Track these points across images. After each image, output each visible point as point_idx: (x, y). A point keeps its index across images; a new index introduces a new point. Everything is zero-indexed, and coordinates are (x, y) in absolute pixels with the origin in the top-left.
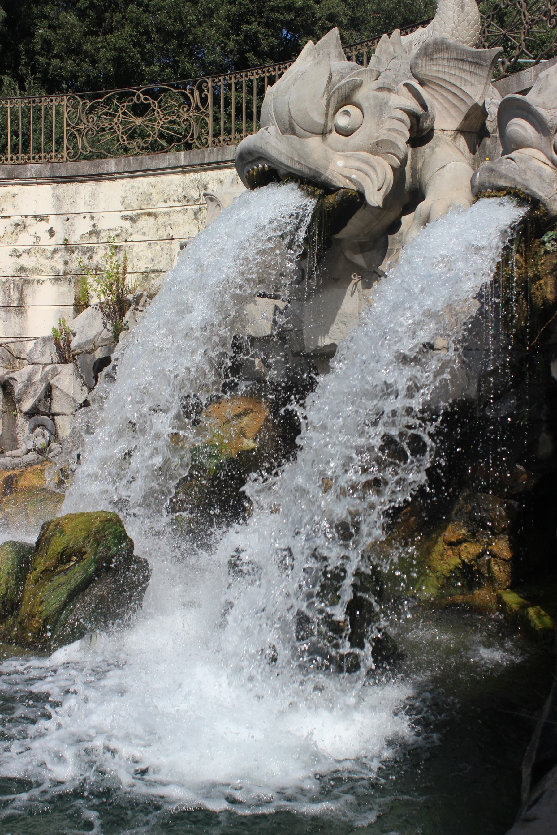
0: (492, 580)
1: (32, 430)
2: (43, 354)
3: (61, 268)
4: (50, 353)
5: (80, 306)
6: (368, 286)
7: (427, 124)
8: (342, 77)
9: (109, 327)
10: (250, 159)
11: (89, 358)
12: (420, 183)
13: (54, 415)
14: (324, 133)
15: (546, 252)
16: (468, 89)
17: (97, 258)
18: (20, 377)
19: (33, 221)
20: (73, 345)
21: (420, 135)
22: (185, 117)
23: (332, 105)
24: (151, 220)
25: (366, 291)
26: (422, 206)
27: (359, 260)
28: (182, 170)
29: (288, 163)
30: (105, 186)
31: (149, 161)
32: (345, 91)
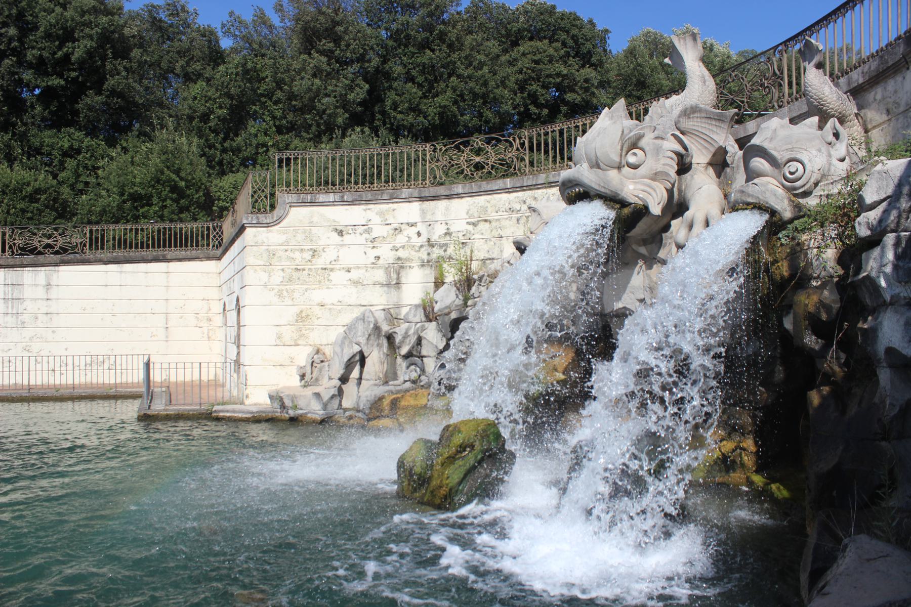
0: (743, 465)
1: (408, 367)
2: (415, 316)
3: (425, 257)
4: (420, 315)
5: (439, 283)
6: (650, 267)
7: (688, 160)
8: (631, 131)
9: (460, 297)
10: (570, 185)
11: (447, 318)
12: (684, 199)
13: (423, 357)
14: (619, 168)
15: (782, 245)
16: (715, 137)
17: (450, 251)
18: (400, 331)
20: (436, 309)
21: (684, 168)
22: (510, 155)
23: (625, 149)
24: (487, 224)
25: (649, 271)
26: (688, 214)
27: (643, 250)
28: (508, 191)
29: (597, 187)
30: (455, 202)
31: (485, 185)
32: (633, 140)
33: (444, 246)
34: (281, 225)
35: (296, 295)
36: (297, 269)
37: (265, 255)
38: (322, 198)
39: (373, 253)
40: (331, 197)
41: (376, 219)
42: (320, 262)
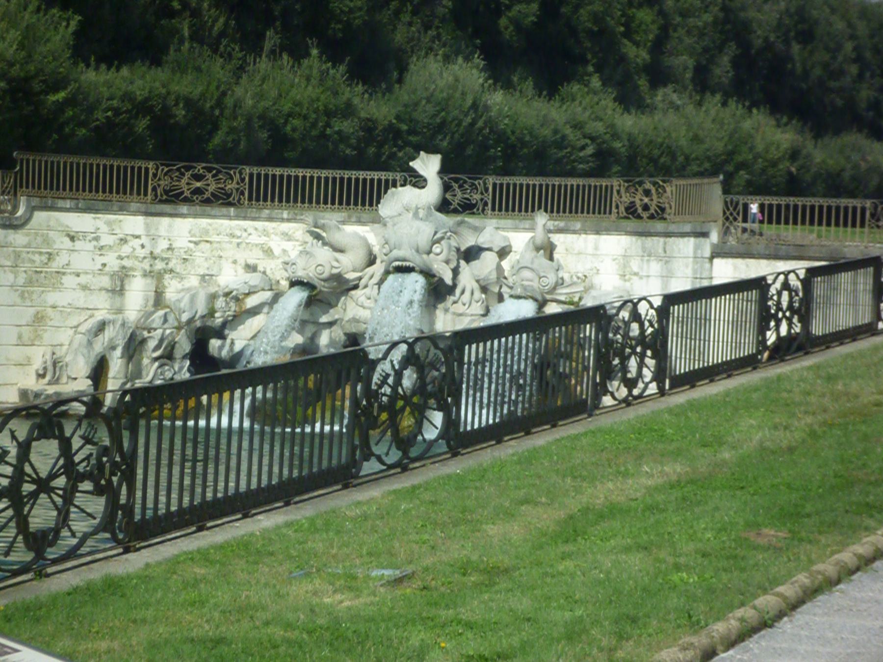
3: (147, 268)
16: (470, 239)
19: (132, 238)
22: (229, 186)
24: (208, 245)
30: (178, 221)
33: (167, 260)
34: (28, 227)
35: (35, 296)
36: (36, 272)
37: (12, 256)
38: (61, 203)
39: (100, 260)
40: (68, 204)
41: (104, 228)
42: (56, 265)
